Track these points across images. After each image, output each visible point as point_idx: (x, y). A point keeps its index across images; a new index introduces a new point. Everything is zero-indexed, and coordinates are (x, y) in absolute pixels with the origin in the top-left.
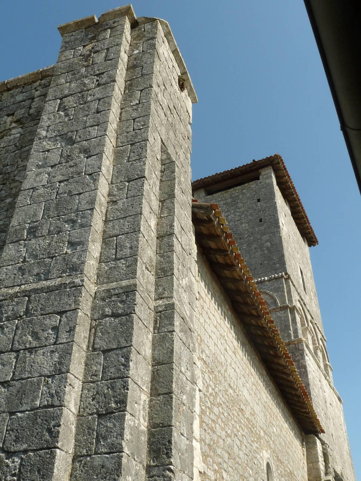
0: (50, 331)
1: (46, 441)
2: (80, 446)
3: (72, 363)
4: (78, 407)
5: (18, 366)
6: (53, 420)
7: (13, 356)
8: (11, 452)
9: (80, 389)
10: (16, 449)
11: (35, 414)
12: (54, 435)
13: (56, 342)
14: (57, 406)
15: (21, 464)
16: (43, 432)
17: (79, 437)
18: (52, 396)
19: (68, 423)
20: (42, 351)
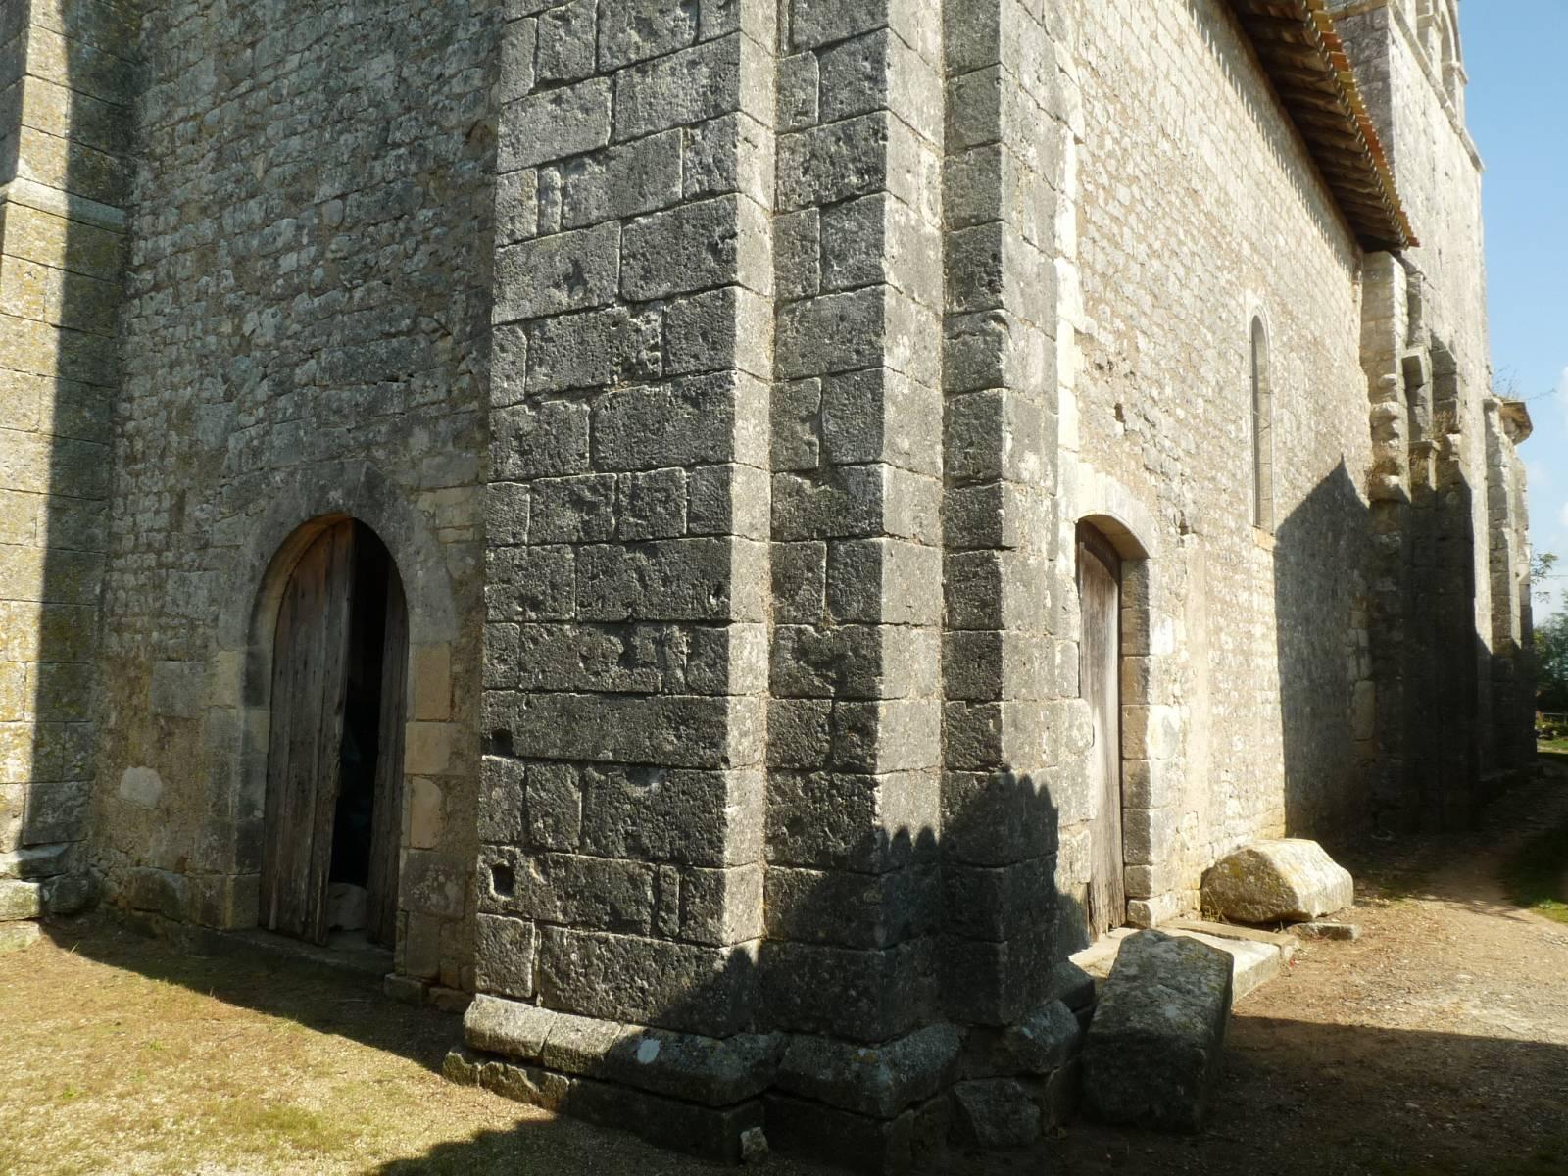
0: (679, 12)
1: (710, 272)
2: (787, 279)
3: (742, 85)
4: (772, 192)
5: (618, 108)
6: (719, 225)
7: (603, 87)
8: (639, 302)
9: (773, 150)
10: (648, 294)
11: (677, 216)
12: (726, 258)
13: (696, 38)
14: (722, 193)
15: (665, 325)
16: (700, 253)
17: (784, 260)
18: (708, 170)
19: (752, 229)
20: (668, 65)
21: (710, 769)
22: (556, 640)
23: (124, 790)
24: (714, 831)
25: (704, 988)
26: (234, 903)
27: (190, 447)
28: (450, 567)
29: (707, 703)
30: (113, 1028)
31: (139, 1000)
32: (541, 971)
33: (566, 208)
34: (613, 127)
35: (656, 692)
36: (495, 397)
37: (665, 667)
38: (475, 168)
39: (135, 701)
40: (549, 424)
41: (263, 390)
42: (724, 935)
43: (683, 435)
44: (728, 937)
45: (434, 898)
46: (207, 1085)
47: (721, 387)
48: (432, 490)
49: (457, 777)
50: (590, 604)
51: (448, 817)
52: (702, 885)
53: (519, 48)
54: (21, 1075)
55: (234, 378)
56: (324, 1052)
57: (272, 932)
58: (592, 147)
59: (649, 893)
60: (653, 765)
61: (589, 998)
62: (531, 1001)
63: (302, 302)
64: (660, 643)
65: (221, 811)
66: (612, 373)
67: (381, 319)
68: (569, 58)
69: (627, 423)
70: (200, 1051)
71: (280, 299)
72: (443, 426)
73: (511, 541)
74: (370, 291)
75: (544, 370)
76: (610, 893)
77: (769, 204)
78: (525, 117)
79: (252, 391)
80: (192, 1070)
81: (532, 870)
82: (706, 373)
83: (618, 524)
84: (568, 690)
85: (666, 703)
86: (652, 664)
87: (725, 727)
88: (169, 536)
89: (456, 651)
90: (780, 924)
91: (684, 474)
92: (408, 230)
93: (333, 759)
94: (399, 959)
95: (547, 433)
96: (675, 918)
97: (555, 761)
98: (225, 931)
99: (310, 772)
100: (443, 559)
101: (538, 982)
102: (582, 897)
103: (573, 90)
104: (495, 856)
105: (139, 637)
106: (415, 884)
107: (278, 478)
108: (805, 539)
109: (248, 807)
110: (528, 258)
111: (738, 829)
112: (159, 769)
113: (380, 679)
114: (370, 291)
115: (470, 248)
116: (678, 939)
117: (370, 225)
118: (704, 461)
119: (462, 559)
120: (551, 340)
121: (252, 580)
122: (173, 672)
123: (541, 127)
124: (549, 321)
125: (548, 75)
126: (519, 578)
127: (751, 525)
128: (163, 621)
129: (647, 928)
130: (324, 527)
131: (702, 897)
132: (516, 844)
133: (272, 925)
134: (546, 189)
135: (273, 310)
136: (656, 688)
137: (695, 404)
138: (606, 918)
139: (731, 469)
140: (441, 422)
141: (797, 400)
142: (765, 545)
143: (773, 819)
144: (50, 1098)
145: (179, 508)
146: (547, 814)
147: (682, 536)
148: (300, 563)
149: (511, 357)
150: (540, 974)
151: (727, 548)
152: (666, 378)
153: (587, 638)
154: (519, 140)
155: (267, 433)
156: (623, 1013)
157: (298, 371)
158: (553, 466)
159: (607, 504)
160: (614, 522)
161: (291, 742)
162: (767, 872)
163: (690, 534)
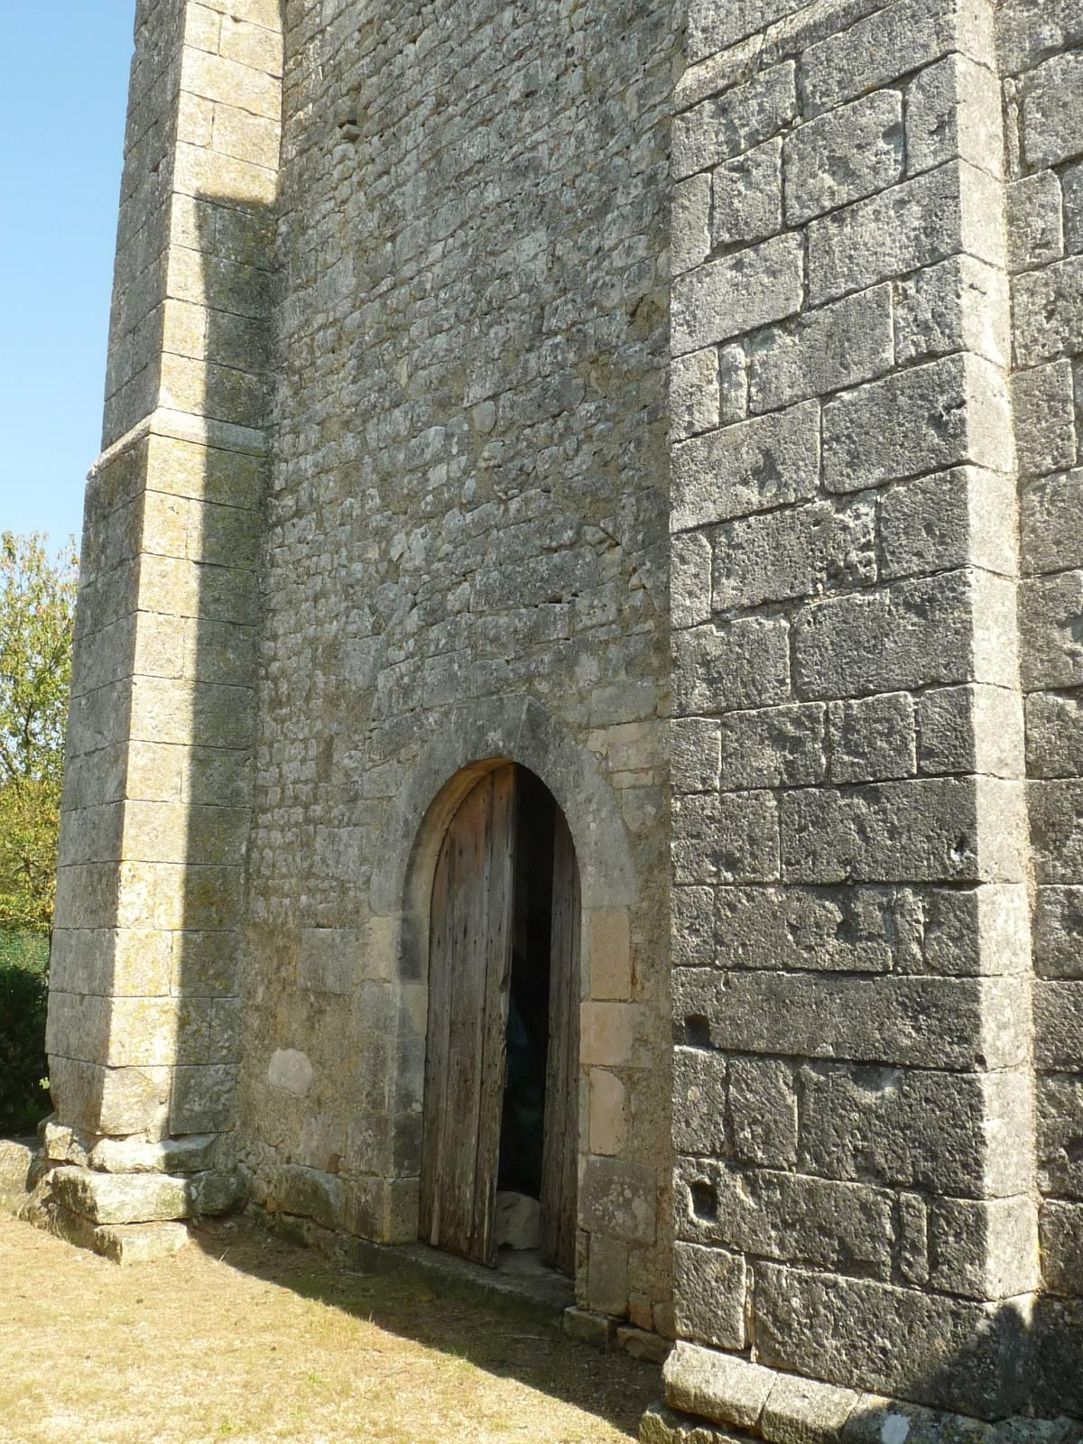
0: (882, 144)
1: (933, 451)
2: (1032, 450)
3: (963, 222)
4: (1008, 346)
5: (812, 266)
6: (942, 393)
7: (793, 244)
8: (845, 494)
9: (1007, 294)
10: (856, 483)
11: (889, 387)
12: (950, 429)
13: (905, 172)
14: (945, 354)
15: (878, 519)
16: (919, 428)
17: (1027, 427)
18: (925, 328)
19: (984, 393)
20: (870, 209)
21: (959, 1071)
22: (758, 907)
23: (272, 1075)
24: (970, 1153)
25: (965, 1354)
26: (392, 1211)
27: (337, 688)
28: (626, 817)
29: (953, 986)
30: (268, 1352)
31: (294, 1321)
32: (755, 1318)
33: (753, 390)
34: (807, 292)
35: (886, 972)
36: (676, 617)
37: (898, 942)
38: (641, 350)
39: (283, 974)
40: (740, 646)
41: (414, 620)
42: (989, 1287)
43: (908, 652)
44: (994, 1289)
45: (620, 1216)
46: (372, 1430)
47: (953, 590)
48: (603, 727)
49: (643, 1070)
50: (798, 862)
51: (632, 1118)
52: (955, 1219)
53: (692, 210)
54: (179, 1401)
55: (382, 609)
56: (500, 1399)
57: (436, 1248)
58: (781, 316)
59: (888, 1226)
60: (885, 1064)
61: (816, 1355)
62: (744, 1354)
63: (454, 520)
64: (889, 909)
65: (376, 1103)
66: (815, 581)
67: (540, 531)
68: (751, 215)
69: (836, 640)
70: (362, 1389)
71: (430, 516)
72: (613, 652)
73: (700, 787)
74: (527, 501)
75: (732, 582)
76: (838, 1224)
77: (1005, 361)
78: (701, 290)
79: (401, 622)
80: (355, 1410)
81: (739, 1191)
82: (933, 573)
83: (829, 763)
84: (774, 968)
85: (900, 985)
86: (880, 936)
87: (977, 1017)
88: (316, 787)
89: (636, 918)
90: (1063, 1275)
91: (910, 699)
92: (568, 428)
93: (499, 1044)
94: (581, 1289)
95: (739, 656)
96: (923, 1260)
97: (763, 1056)
98: (383, 1244)
99: (473, 1058)
100: (618, 807)
101: (752, 1331)
102: (802, 1227)
103: (756, 251)
104: (694, 1171)
105: (287, 901)
106: (597, 1199)
107: (432, 718)
108: (1072, 775)
109: (405, 1099)
110: (709, 453)
111: (1000, 1149)
112: (309, 1052)
113: (548, 948)
114: (527, 501)
115: (639, 443)
116: (928, 1288)
117: (525, 427)
118: (936, 683)
119: (641, 807)
120: (740, 546)
121: (405, 836)
122: (323, 940)
123: (720, 299)
124: (736, 524)
125: (726, 237)
126: (711, 831)
127: (1001, 761)
128: (312, 883)
129: (887, 1272)
130: (483, 773)
131: (957, 1235)
132: (718, 1157)
133: (434, 1239)
134: (729, 370)
135: (422, 529)
136: (886, 966)
137: (921, 612)
138: (834, 1256)
139: (971, 692)
140: (613, 648)
141: (1053, 599)
142: (1021, 784)
143: (1046, 1138)
144: (209, 1430)
145: (327, 755)
146: (755, 1122)
147: (912, 776)
148: (457, 815)
149: (693, 570)
150: (753, 1320)
151: (971, 791)
152: (883, 583)
153: (796, 904)
154: (695, 317)
155: (418, 668)
156: (861, 1379)
157: (450, 597)
158: (747, 696)
159: (814, 740)
160: (824, 760)
161: (452, 1023)
162: (1041, 1208)
163: (922, 773)
